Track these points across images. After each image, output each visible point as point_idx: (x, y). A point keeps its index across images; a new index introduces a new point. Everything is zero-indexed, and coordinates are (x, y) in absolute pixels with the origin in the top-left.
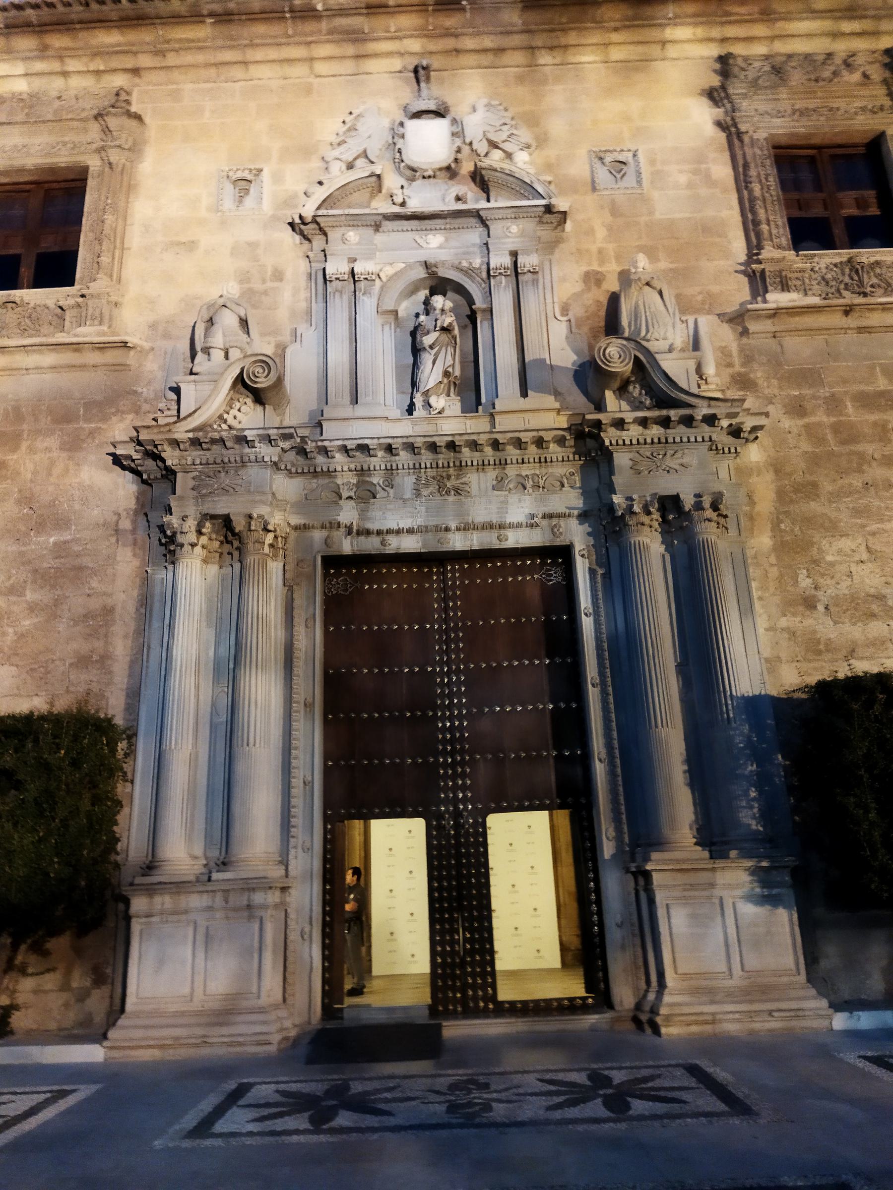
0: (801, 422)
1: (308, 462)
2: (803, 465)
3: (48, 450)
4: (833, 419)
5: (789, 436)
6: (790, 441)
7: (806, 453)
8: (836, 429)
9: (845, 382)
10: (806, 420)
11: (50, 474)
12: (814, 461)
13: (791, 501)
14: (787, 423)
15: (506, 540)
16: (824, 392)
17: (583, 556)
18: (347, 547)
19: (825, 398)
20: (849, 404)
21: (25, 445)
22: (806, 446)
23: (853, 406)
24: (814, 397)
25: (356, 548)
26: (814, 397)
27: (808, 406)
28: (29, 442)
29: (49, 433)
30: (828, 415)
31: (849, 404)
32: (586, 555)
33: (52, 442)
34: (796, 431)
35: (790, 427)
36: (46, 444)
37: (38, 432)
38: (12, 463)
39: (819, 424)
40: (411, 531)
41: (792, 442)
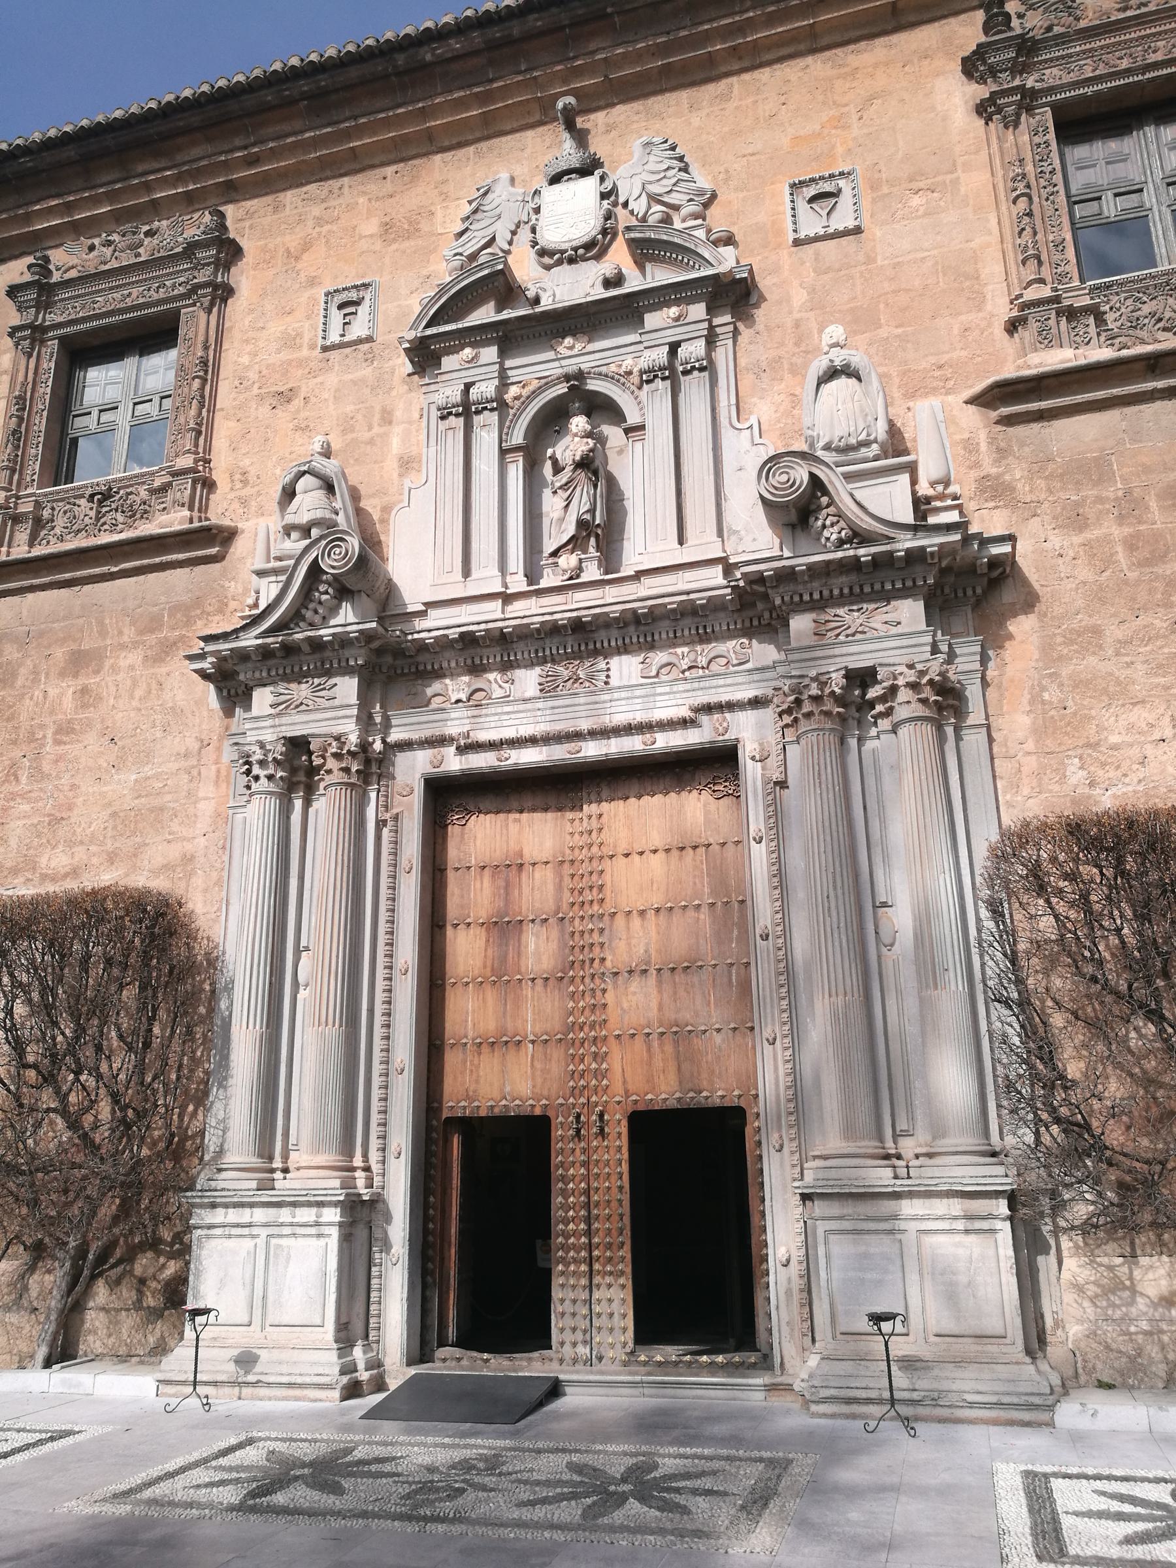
0: (1077, 539)
1: (410, 660)
2: (1080, 603)
3: (132, 667)
4: (1127, 530)
5: (1060, 561)
6: (1062, 568)
7: (1084, 583)
8: (1131, 545)
9: (1147, 469)
10: (1088, 535)
11: (132, 697)
12: (1098, 596)
13: (1060, 658)
14: (1056, 541)
15: (654, 743)
16: (1114, 490)
17: (753, 758)
18: (454, 763)
19: (1117, 499)
20: (1153, 505)
21: (108, 663)
22: (1085, 573)
23: (1160, 508)
24: (1100, 500)
25: (465, 767)
26: (1100, 500)
27: (1090, 512)
28: (112, 661)
29: (135, 645)
30: (1120, 525)
31: (1153, 505)
32: (758, 758)
33: (133, 658)
34: (1071, 554)
35: (1061, 547)
36: (128, 662)
37: (123, 647)
38: (94, 687)
39: (1107, 540)
40: (532, 741)
41: (1063, 567)
